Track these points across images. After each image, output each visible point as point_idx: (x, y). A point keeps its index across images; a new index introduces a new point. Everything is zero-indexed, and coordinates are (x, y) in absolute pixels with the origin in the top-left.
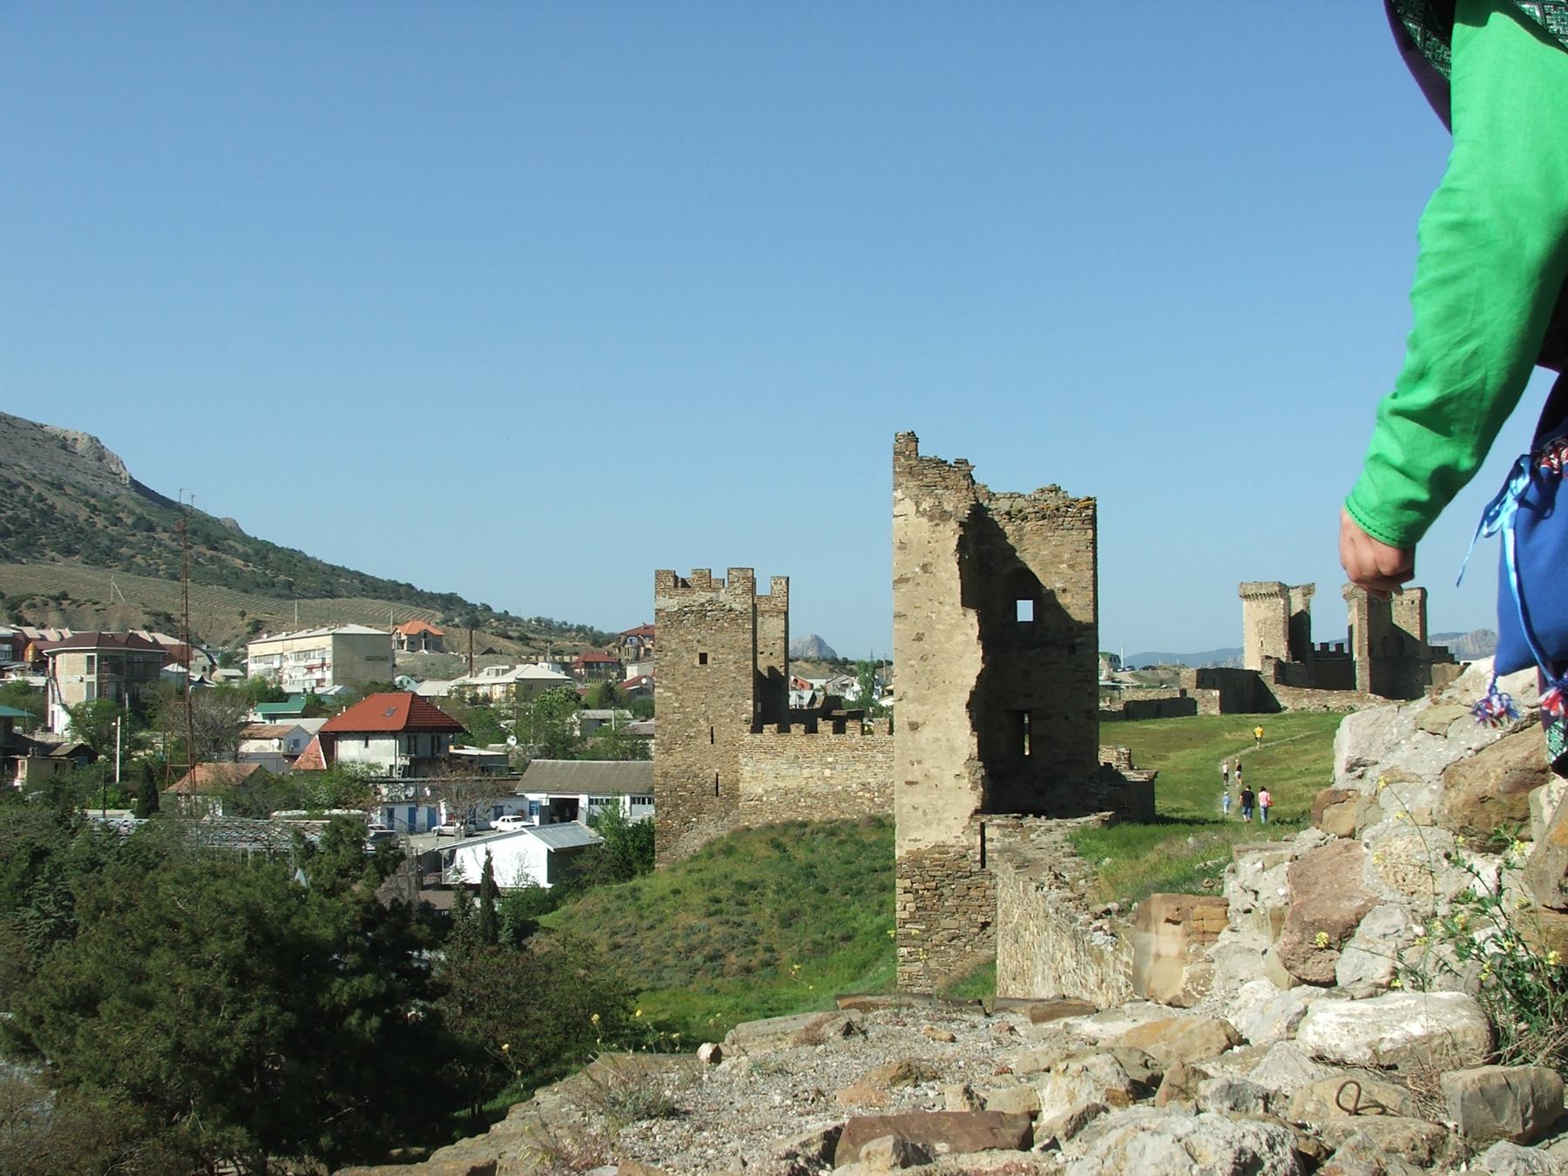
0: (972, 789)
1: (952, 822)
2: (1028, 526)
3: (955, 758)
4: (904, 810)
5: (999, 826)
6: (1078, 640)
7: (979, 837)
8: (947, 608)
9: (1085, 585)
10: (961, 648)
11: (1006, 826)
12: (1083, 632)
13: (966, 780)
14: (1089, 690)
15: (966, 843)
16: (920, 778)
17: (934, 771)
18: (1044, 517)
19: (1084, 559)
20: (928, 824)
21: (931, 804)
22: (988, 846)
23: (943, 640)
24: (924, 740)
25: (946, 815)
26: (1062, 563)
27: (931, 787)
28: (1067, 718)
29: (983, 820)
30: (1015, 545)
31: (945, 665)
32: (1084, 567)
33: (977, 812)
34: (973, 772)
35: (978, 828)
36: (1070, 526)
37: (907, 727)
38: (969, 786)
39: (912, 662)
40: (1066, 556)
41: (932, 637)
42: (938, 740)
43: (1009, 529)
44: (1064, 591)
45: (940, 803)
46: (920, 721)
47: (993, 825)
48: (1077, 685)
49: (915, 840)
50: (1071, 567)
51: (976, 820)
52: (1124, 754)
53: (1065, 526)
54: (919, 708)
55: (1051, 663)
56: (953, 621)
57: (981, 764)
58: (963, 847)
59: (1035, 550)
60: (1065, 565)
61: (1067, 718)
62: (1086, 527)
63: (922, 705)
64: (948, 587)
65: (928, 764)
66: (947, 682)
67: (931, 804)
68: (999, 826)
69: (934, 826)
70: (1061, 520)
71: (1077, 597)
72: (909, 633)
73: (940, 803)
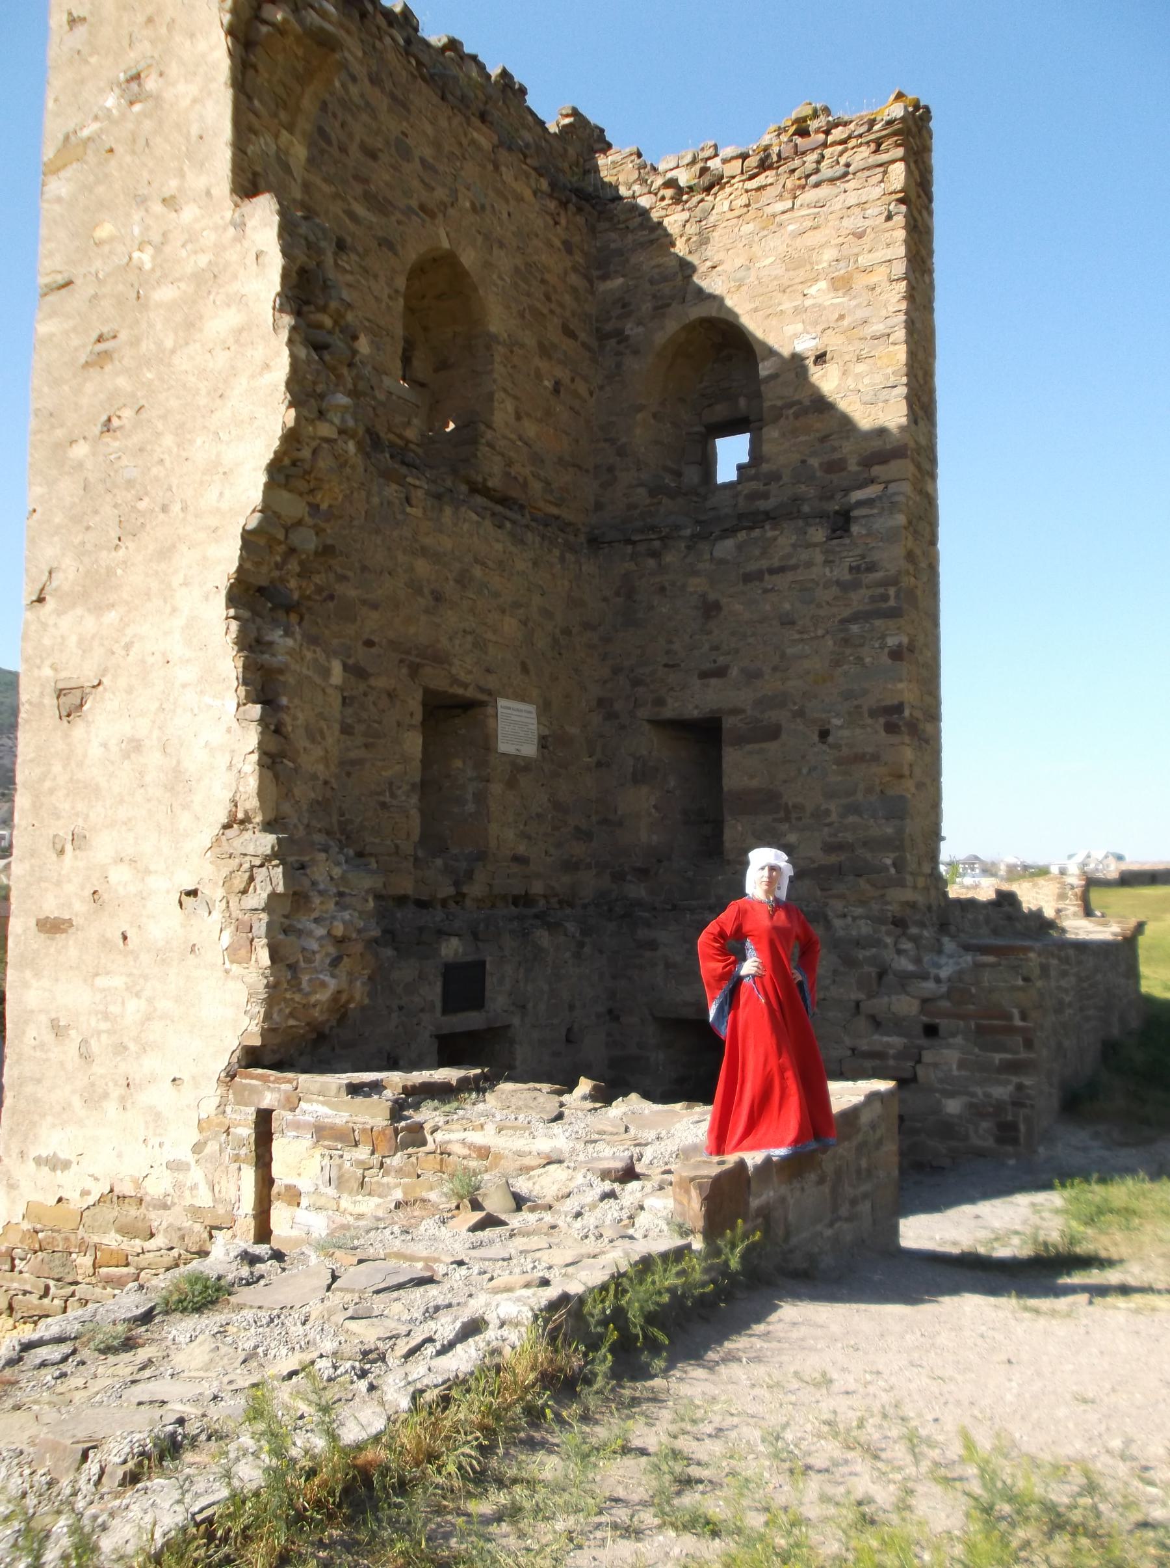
0: (232, 952)
1: (160, 1096)
2: (721, 202)
3: (185, 820)
4: (31, 1032)
5: (321, 1132)
6: (857, 495)
7: (249, 1175)
8: (189, 213)
9: (879, 328)
10: (221, 360)
11: (347, 1137)
12: (876, 470)
13: (217, 915)
14: (891, 641)
15: (204, 1199)
16: (79, 908)
17: (120, 875)
18: (765, 165)
19: (882, 254)
20: (93, 1098)
21: (106, 1016)
22: (279, 1216)
23: (169, 343)
24: (95, 751)
25: (150, 1063)
26: (816, 280)
27: (105, 943)
28: (824, 734)
29: (268, 1100)
30: (690, 258)
31: (168, 440)
32: (879, 276)
33: (252, 1058)
34: (239, 881)
35: (246, 1131)
36: (839, 170)
37: (50, 701)
38: (227, 938)
39: (81, 450)
40: (829, 254)
41: (135, 342)
42: (134, 746)
43: (674, 220)
44: (821, 358)
45: (134, 1007)
46: (86, 674)
47: (297, 1126)
48: (855, 628)
49: (56, 1164)
50: (842, 284)
51: (240, 1102)
52: (1072, 887)
53: (826, 171)
54: (90, 623)
55: (782, 570)
56: (203, 260)
57: (267, 842)
58: (195, 1212)
59: (739, 262)
60: (823, 284)
61: (824, 734)
62: (884, 157)
63: (99, 609)
64: (195, 131)
65: (104, 847)
66: (176, 508)
67: (106, 1016)
68: (321, 1132)
69: (111, 1107)
70: (812, 157)
71: (860, 368)
72: (75, 341)
73: (134, 1007)
